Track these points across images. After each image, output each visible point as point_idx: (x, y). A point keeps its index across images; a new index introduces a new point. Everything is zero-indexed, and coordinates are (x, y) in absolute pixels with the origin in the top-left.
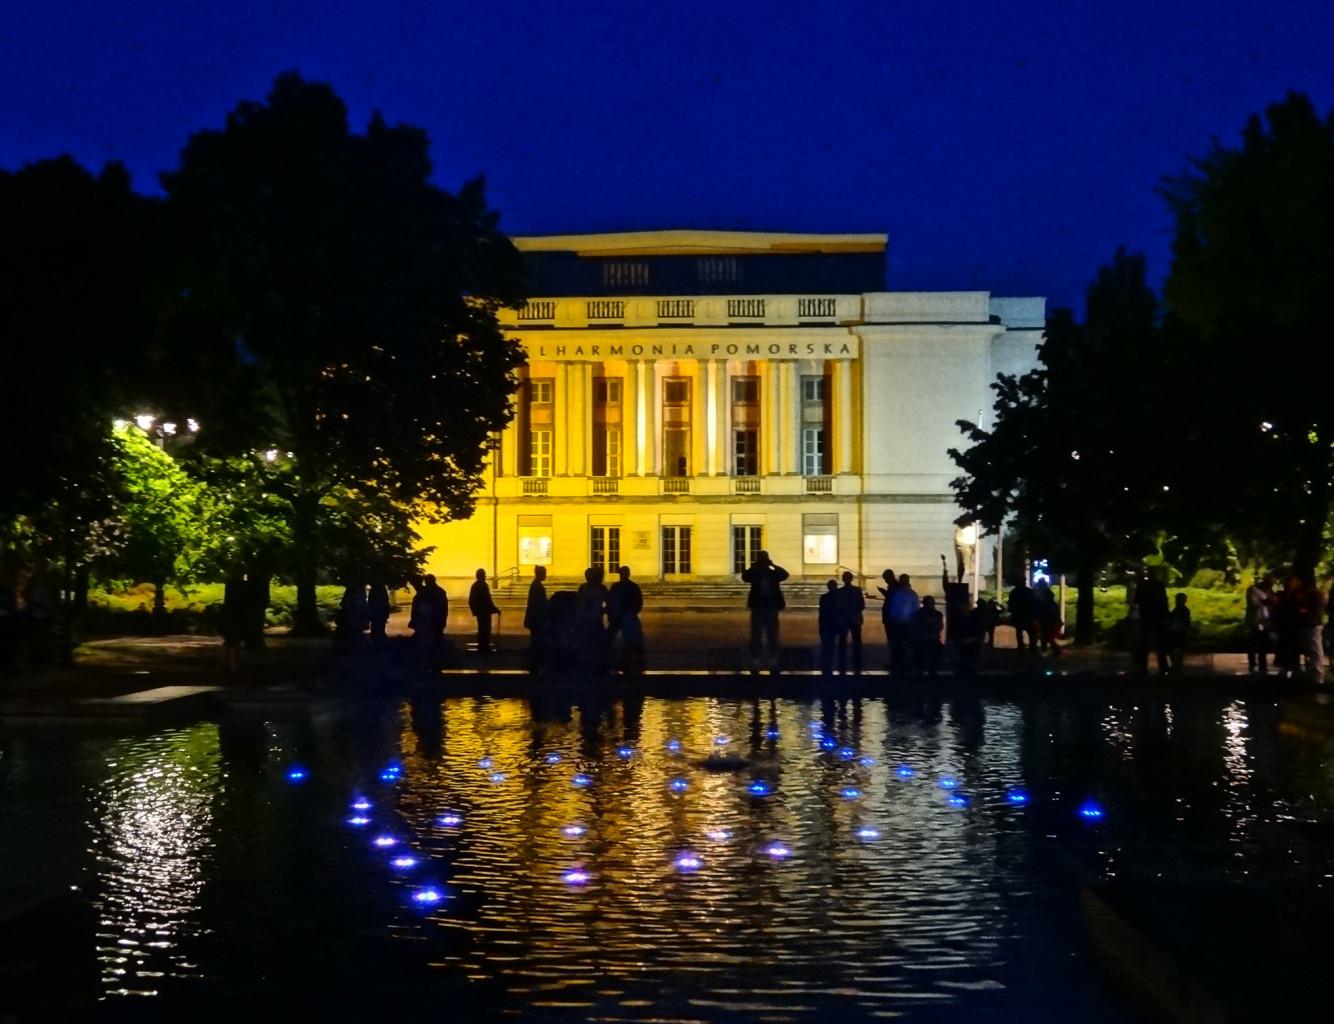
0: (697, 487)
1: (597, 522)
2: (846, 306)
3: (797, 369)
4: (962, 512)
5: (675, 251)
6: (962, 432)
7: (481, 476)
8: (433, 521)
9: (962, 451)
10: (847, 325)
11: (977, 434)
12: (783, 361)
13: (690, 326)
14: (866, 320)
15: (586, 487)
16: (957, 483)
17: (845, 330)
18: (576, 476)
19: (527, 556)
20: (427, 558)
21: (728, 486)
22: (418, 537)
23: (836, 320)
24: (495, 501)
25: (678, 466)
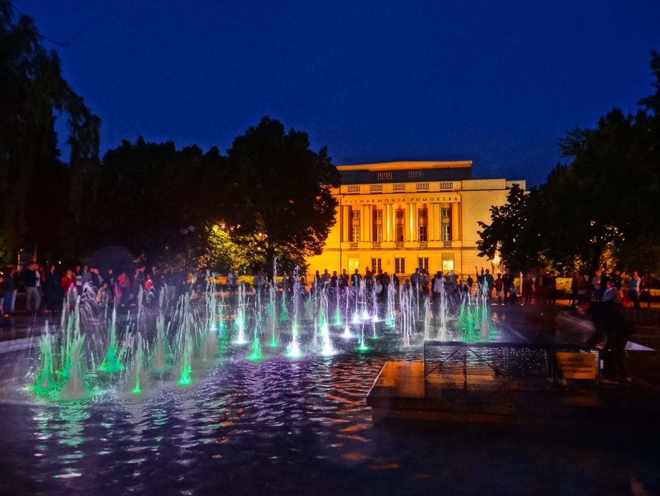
0: (406, 245)
1: (373, 257)
2: (456, 185)
3: (440, 207)
4: (480, 252)
5: (355, 169)
6: (480, 225)
7: (325, 242)
8: (308, 256)
9: (482, 232)
10: (457, 191)
11: (484, 226)
12: (435, 203)
13: (404, 193)
14: (463, 189)
15: (370, 245)
16: (478, 242)
17: (456, 193)
18: (367, 242)
19: (351, 268)
20: (308, 267)
21: (417, 245)
22: (305, 261)
23: (453, 190)
24: (341, 250)
25: (400, 238)
